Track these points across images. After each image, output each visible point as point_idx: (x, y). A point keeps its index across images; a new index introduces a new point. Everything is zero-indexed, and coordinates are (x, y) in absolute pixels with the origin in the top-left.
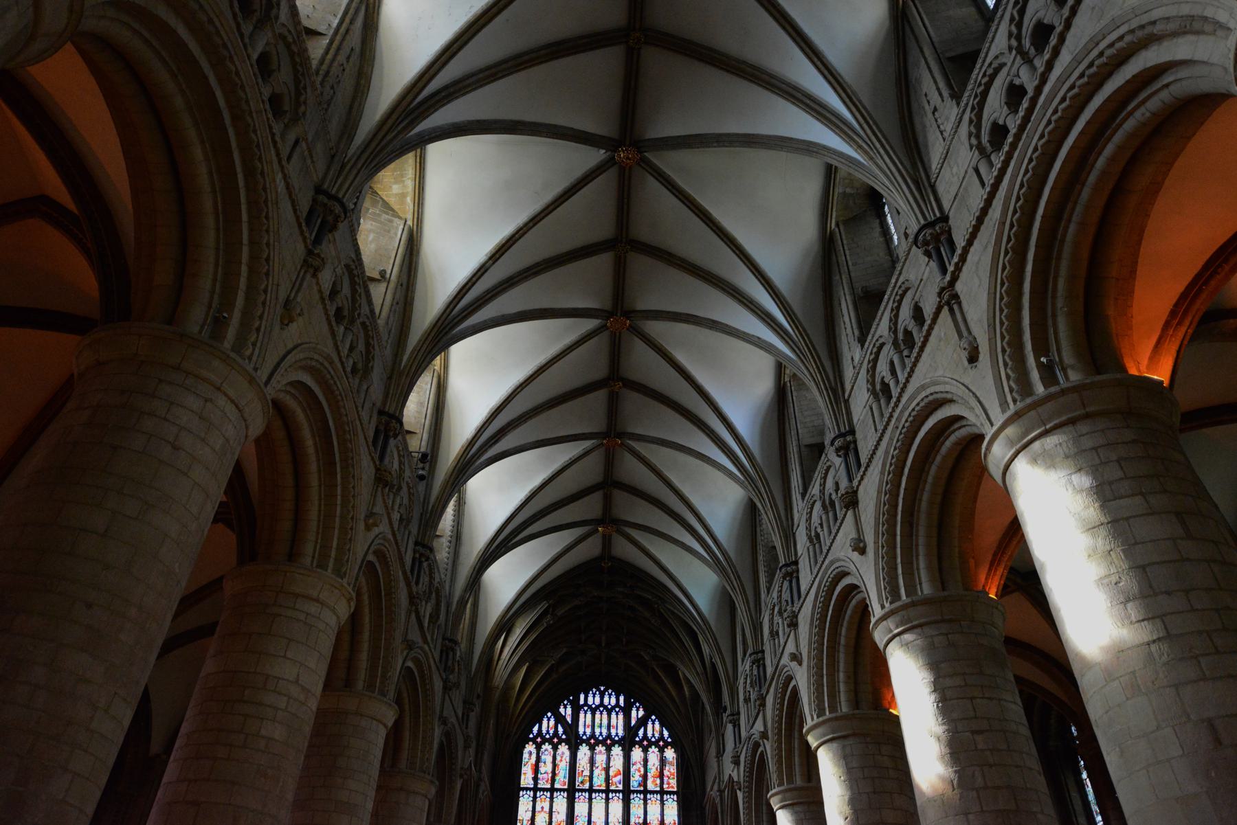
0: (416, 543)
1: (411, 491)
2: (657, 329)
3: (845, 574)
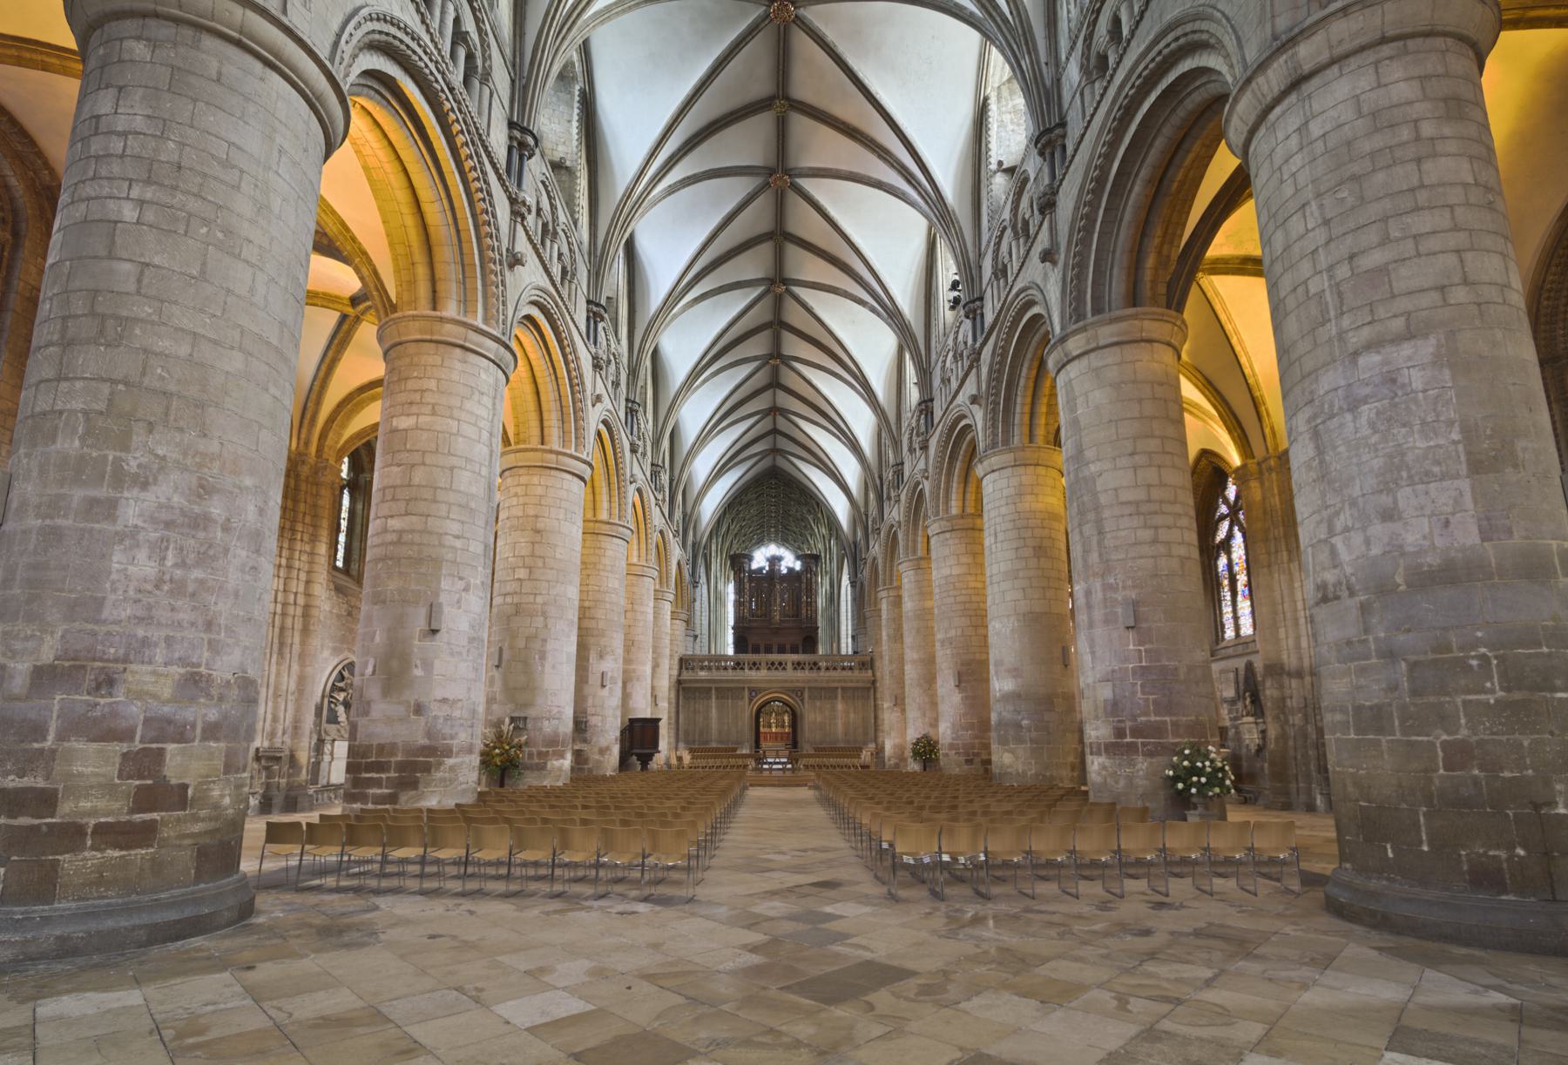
0: (627, 400)
2: (817, 189)
3: (964, 417)
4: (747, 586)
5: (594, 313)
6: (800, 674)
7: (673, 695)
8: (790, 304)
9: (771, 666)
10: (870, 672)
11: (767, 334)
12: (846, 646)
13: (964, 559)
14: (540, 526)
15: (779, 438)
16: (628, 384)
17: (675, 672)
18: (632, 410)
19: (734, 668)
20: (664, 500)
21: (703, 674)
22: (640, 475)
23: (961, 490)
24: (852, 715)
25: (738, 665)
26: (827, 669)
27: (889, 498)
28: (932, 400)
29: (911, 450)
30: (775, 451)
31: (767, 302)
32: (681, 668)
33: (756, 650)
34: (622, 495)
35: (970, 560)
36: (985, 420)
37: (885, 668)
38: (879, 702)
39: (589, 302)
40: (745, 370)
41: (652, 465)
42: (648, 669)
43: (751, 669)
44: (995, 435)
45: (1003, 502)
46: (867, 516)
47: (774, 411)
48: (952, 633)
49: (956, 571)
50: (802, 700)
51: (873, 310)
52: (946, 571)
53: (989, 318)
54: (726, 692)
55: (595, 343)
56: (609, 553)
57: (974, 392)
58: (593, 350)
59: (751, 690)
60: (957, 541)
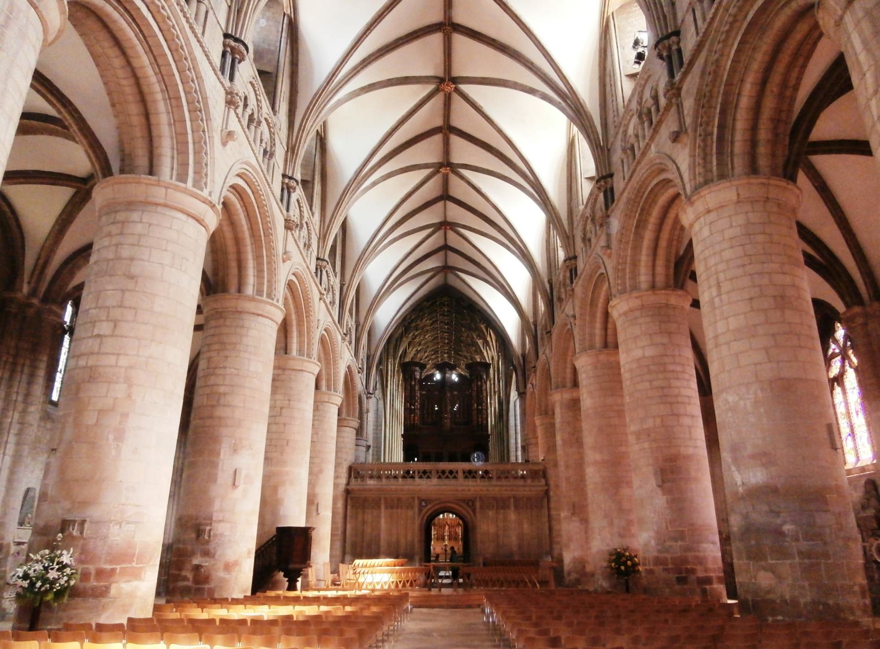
0: (284, 176)
1: (272, 130)
4: (418, 394)
5: (232, 48)
6: (470, 482)
7: (340, 504)
8: (458, 102)
9: (442, 474)
10: (543, 482)
11: (438, 138)
12: (517, 455)
13: (658, 339)
14: (135, 269)
15: (450, 254)
16: (286, 160)
17: (343, 481)
18: (289, 188)
19: (404, 477)
20: (333, 303)
21: (371, 483)
22: (296, 257)
23: (650, 264)
24: (526, 526)
25: (407, 475)
26: (499, 478)
27: (560, 299)
28: (611, 176)
29: (586, 240)
30: (446, 269)
31: (439, 99)
32: (350, 476)
33: (425, 458)
34: (272, 272)
35: (665, 340)
36: (693, 156)
37: (561, 476)
38: (553, 512)
39: (226, 36)
40: (417, 177)
41: (318, 259)
42: (303, 473)
43: (421, 477)
44: (708, 170)
45: (726, 245)
46: (536, 326)
47: (445, 225)
48: (650, 423)
49: (650, 352)
50: (474, 511)
51: (545, 97)
52: (638, 353)
53: (689, 42)
54: (394, 503)
55: (231, 78)
56: (253, 333)
57: (675, 128)
58: (227, 83)
59: (421, 500)
60: (648, 319)
